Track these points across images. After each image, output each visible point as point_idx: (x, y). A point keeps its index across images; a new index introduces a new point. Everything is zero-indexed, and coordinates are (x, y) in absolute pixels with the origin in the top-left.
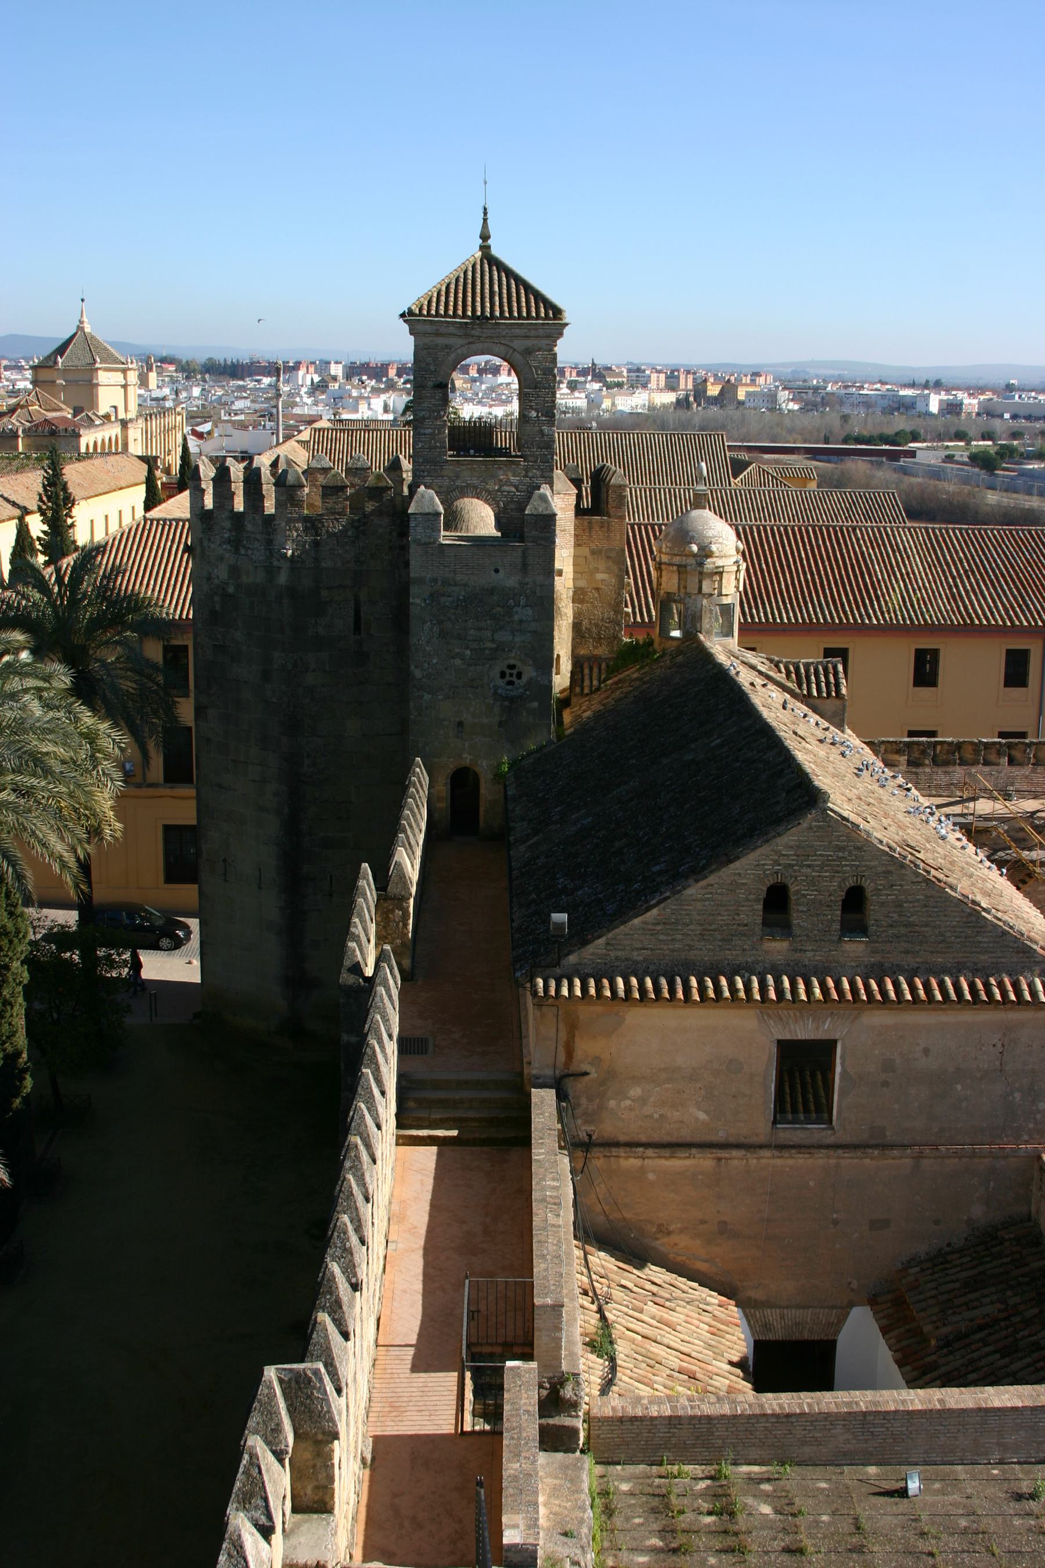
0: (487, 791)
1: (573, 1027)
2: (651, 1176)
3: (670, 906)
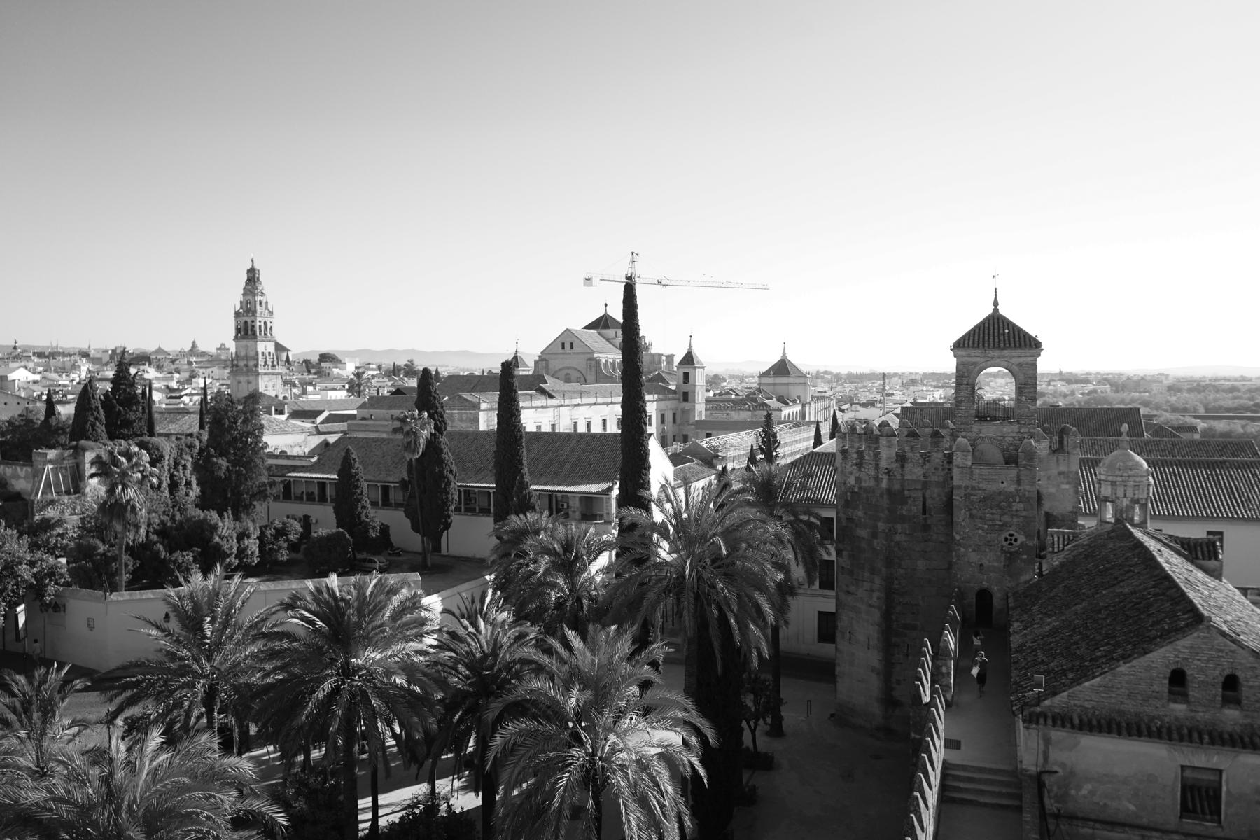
0: (997, 602)
3: (1109, 676)
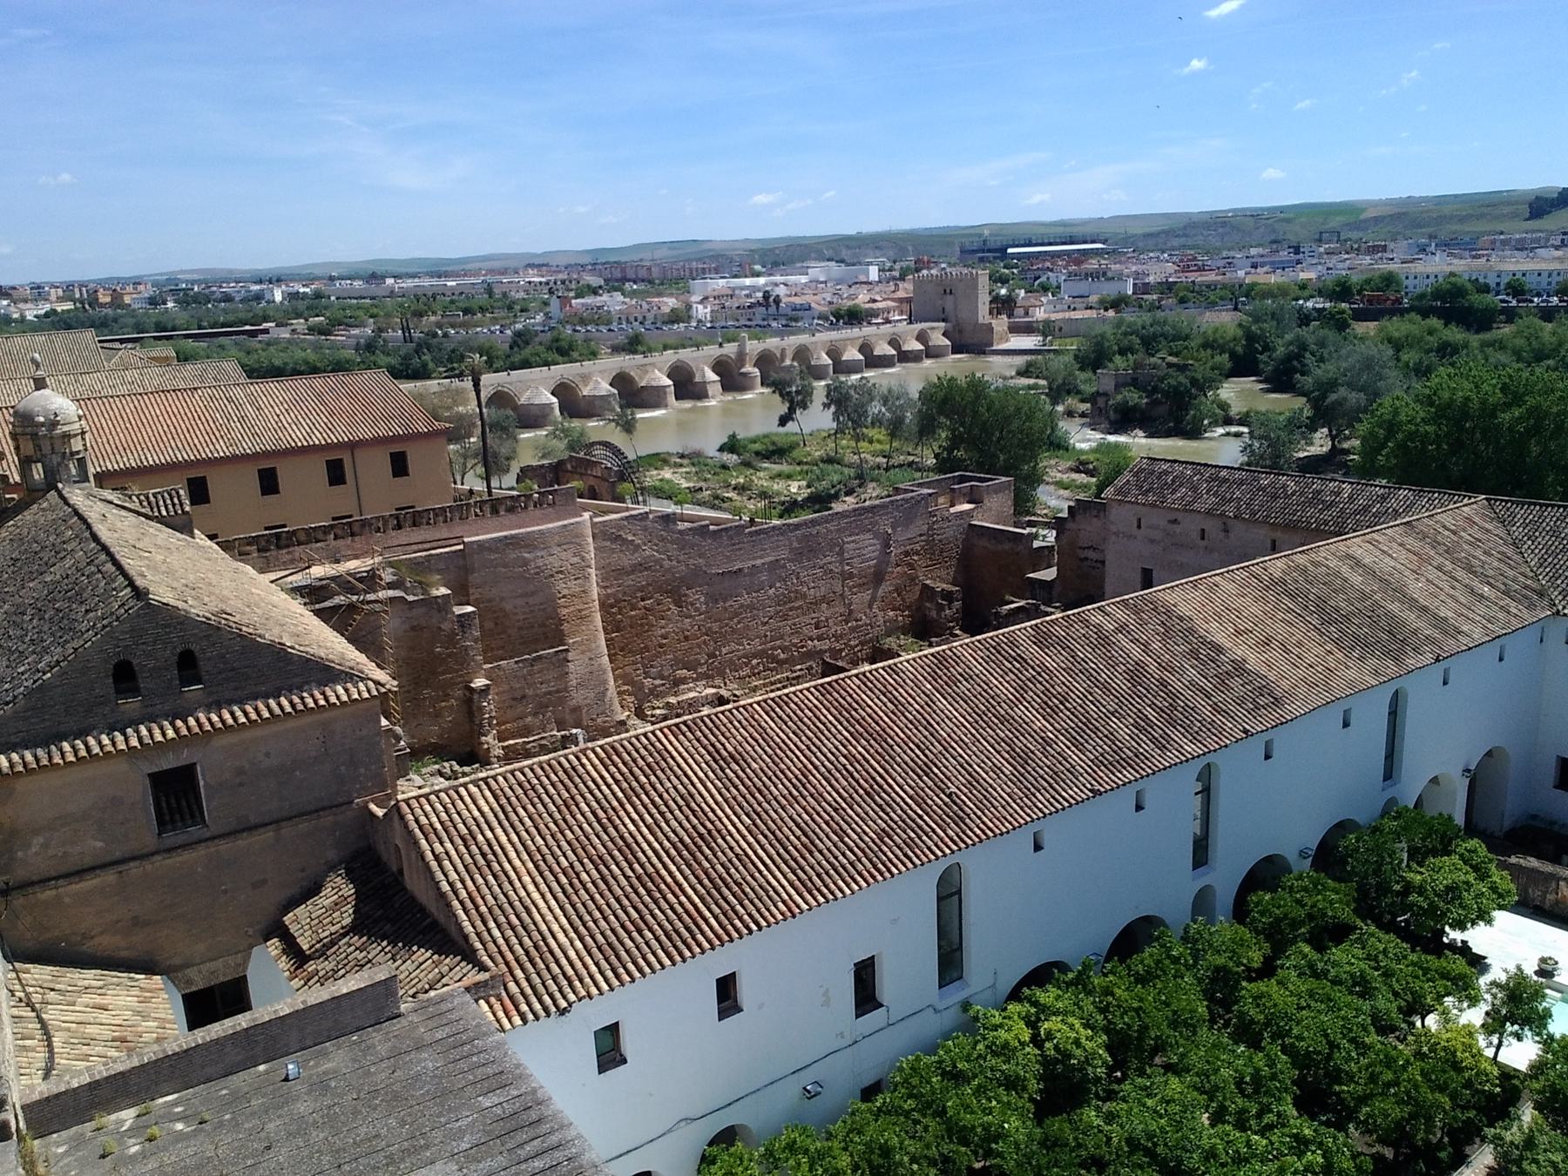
2: (67, 900)
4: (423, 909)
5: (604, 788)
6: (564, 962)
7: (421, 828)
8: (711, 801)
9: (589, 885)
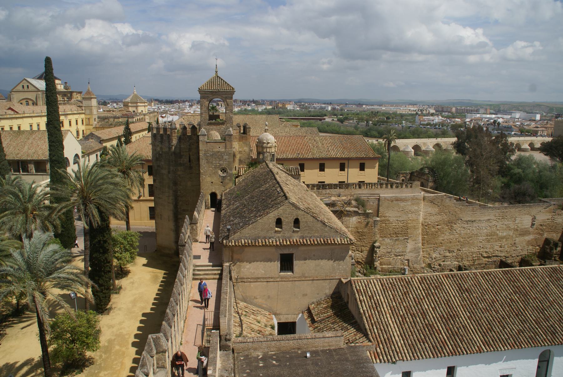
1: (233, 252)
4: (353, 316)
5: (419, 291)
6: (396, 346)
7: (357, 290)
8: (456, 304)
9: (409, 323)
